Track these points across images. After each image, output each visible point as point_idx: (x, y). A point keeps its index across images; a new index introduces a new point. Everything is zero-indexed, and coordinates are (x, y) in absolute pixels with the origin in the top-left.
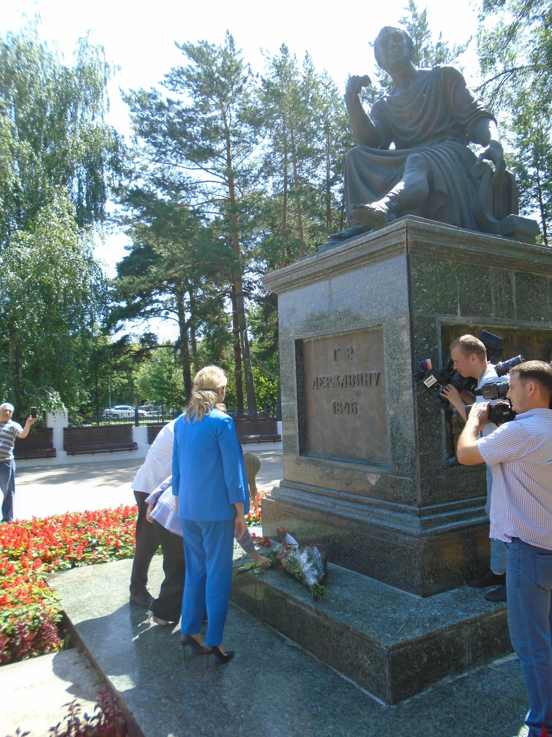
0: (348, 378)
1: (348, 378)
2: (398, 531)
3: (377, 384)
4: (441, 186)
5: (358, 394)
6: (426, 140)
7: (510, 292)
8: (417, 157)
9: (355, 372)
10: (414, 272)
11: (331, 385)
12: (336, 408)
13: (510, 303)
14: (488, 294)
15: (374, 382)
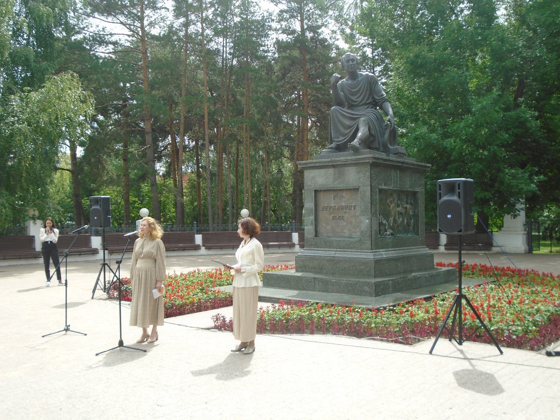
0: (341, 207)
1: (341, 207)
2: (365, 258)
3: (354, 209)
4: (373, 133)
5: (345, 212)
6: (362, 105)
7: (397, 177)
8: (364, 120)
9: (343, 204)
10: (372, 172)
11: (332, 209)
12: (334, 218)
13: (397, 181)
14: (391, 178)
15: (353, 208)
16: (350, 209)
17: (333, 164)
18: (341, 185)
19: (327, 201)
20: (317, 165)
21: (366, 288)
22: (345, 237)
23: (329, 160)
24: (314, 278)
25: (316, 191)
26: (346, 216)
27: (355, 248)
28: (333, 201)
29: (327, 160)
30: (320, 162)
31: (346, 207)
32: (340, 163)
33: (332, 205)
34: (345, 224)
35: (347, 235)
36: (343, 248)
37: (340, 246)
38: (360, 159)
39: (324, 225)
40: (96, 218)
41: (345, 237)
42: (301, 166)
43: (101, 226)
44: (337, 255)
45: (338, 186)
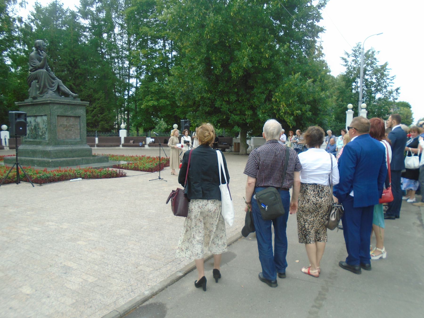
5: (72, 127)
9: (71, 123)
16: (75, 126)
17: (70, 103)
18: (72, 114)
19: (64, 121)
20: (61, 102)
21: (106, 159)
22: (73, 139)
23: (69, 101)
24: (82, 159)
25: (58, 116)
26: (73, 129)
27: (79, 144)
28: (65, 122)
29: (67, 101)
30: (63, 101)
31: (73, 125)
32: (73, 103)
33: (65, 123)
34: (72, 133)
35: (73, 138)
36: (74, 144)
37: (72, 144)
38: (83, 103)
39: (61, 133)
40: (21, 128)
41: (73, 139)
42: (51, 102)
43: (16, 135)
44: (73, 148)
45: (70, 114)
